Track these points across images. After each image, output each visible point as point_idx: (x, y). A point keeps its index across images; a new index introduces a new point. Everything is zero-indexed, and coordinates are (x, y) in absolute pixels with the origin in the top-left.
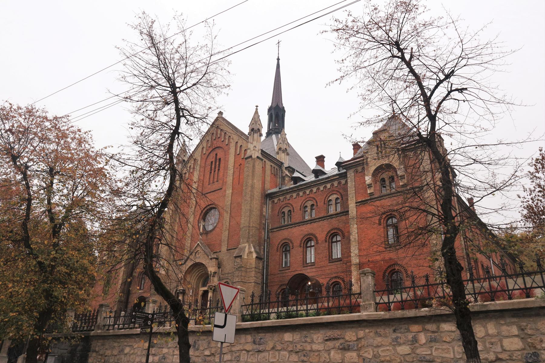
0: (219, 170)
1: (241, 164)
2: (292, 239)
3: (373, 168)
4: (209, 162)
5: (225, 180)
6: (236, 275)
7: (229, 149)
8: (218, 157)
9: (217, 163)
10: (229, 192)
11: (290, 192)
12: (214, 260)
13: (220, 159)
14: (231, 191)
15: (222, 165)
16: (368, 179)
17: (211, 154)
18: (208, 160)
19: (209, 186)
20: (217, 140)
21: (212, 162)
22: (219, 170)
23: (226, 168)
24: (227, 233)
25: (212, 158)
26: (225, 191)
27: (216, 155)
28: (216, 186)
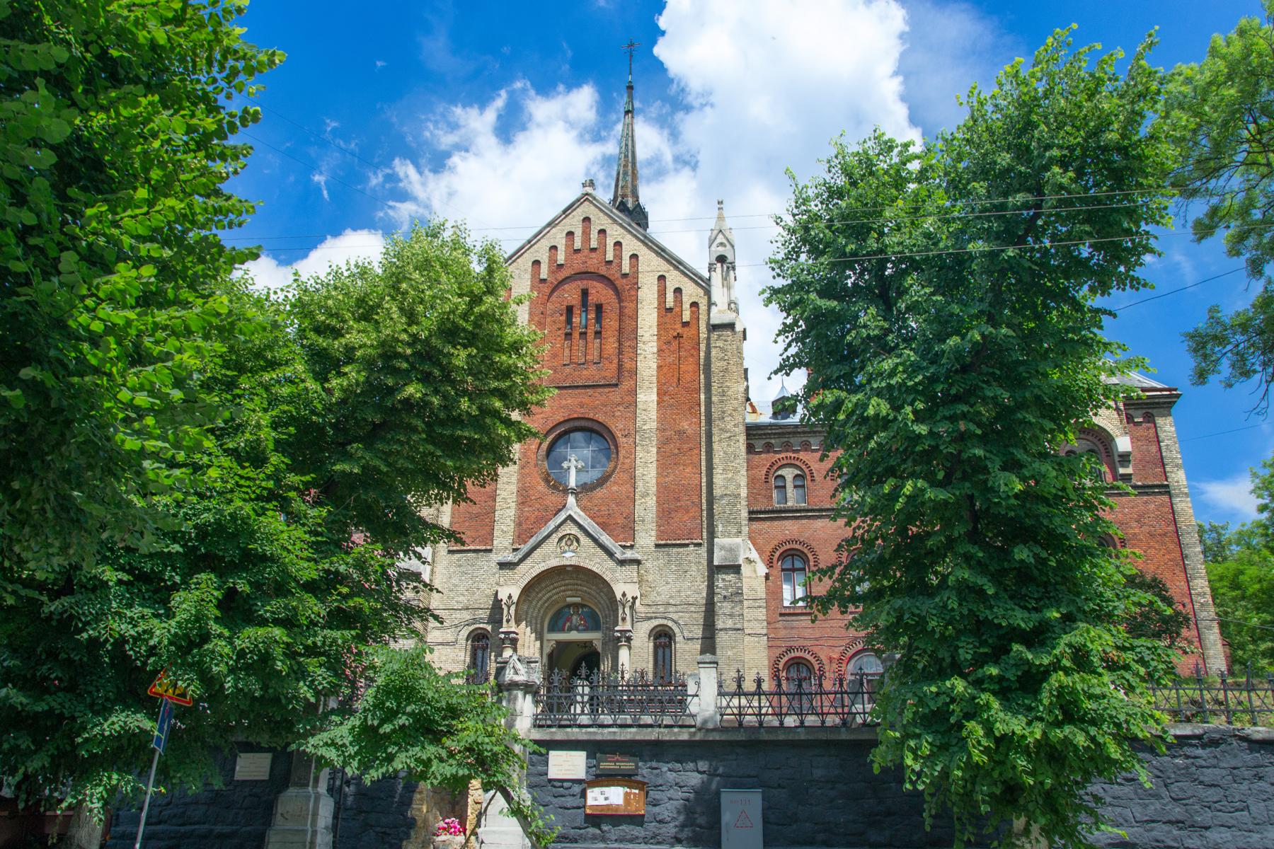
1: (679, 336)
2: (814, 544)
5: (628, 365)
6: (728, 611)
7: (636, 287)
8: (592, 299)
10: (648, 398)
13: (599, 308)
14: (654, 397)
15: (611, 323)
18: (553, 298)
21: (570, 310)
23: (627, 334)
24: (651, 502)
25: (571, 294)
26: (633, 392)
27: (585, 293)
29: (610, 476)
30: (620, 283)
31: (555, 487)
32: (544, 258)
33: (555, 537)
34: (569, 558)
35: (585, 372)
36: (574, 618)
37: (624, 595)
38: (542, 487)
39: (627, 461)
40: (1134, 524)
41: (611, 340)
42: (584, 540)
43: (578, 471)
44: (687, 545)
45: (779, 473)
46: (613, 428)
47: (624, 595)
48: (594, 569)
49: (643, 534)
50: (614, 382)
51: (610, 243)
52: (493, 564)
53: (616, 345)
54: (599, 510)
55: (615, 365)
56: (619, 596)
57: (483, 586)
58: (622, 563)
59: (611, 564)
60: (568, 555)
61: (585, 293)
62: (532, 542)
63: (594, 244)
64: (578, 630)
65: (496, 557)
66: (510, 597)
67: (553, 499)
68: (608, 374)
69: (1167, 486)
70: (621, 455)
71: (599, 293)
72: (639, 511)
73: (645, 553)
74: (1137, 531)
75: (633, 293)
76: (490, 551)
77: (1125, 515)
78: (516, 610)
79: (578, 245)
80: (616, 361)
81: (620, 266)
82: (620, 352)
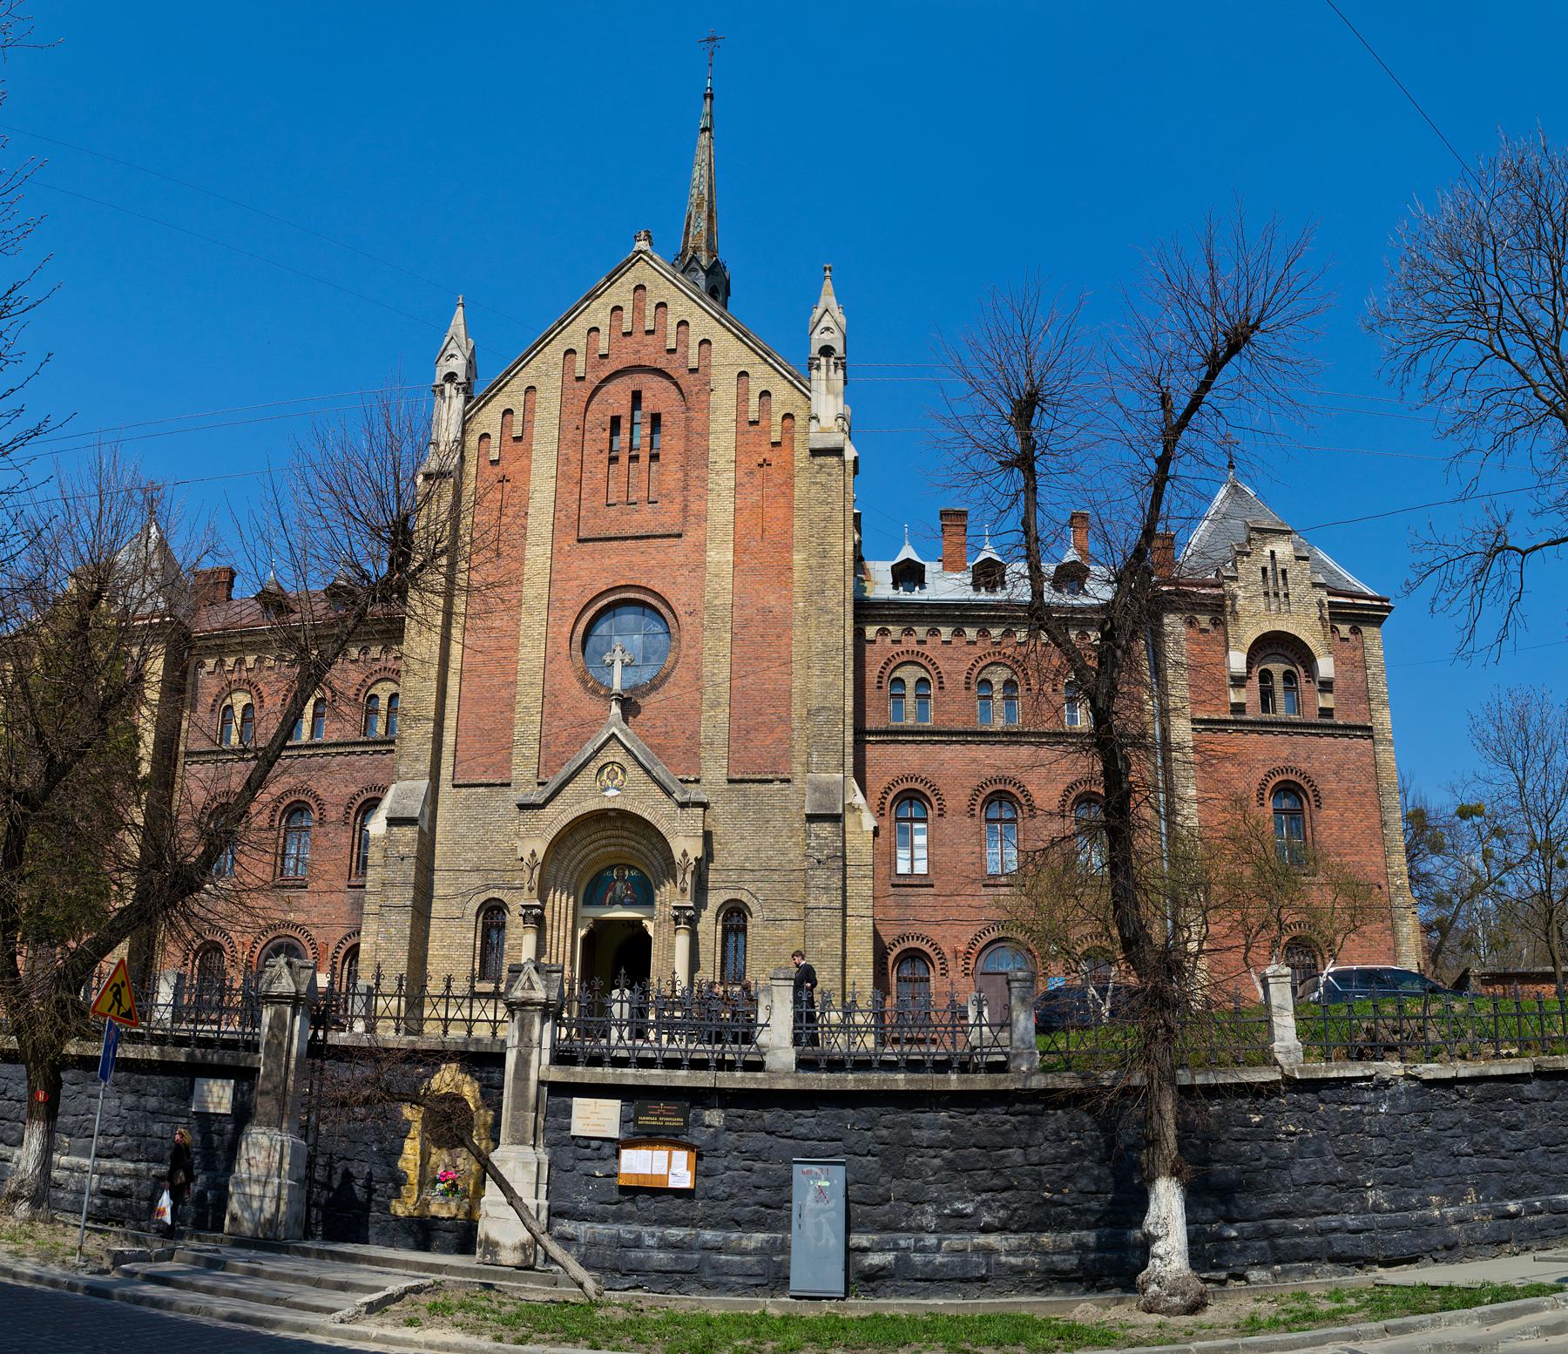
0: (654, 457)
3: (1251, 635)
4: (600, 413)
6: (820, 882)
8: (648, 405)
9: (643, 431)
11: (932, 616)
12: (700, 811)
13: (656, 419)
15: (670, 442)
16: (1237, 661)
17: (610, 387)
18: (593, 405)
19: (612, 512)
20: (638, 336)
22: (654, 457)
23: (696, 459)
24: (723, 715)
25: (617, 398)
27: (637, 397)
28: (644, 519)
29: (667, 676)
30: (686, 381)
31: (595, 692)
32: (579, 343)
33: (593, 767)
34: (612, 798)
35: (636, 516)
36: (619, 885)
37: (685, 854)
38: (576, 689)
39: (693, 652)
40: (1332, 777)
41: (673, 467)
42: (634, 772)
43: (625, 666)
44: (771, 781)
45: (897, 674)
46: (673, 603)
47: (685, 854)
48: (646, 815)
49: (711, 764)
50: (676, 531)
51: (672, 322)
52: (512, 806)
53: (680, 475)
54: (654, 726)
55: (677, 507)
56: (677, 856)
57: (498, 837)
58: (683, 805)
59: (669, 807)
60: (612, 793)
61: (637, 397)
62: (564, 773)
63: (649, 326)
64: (622, 903)
65: (515, 796)
66: (533, 854)
67: (590, 706)
68: (666, 519)
69: (1370, 728)
70: (684, 643)
71: (657, 395)
72: (705, 729)
73: (714, 793)
74: (1334, 786)
75: (703, 398)
76: (508, 785)
77: (1322, 763)
78: (541, 875)
79: (627, 327)
80: (679, 499)
81: (686, 357)
82: (685, 488)
